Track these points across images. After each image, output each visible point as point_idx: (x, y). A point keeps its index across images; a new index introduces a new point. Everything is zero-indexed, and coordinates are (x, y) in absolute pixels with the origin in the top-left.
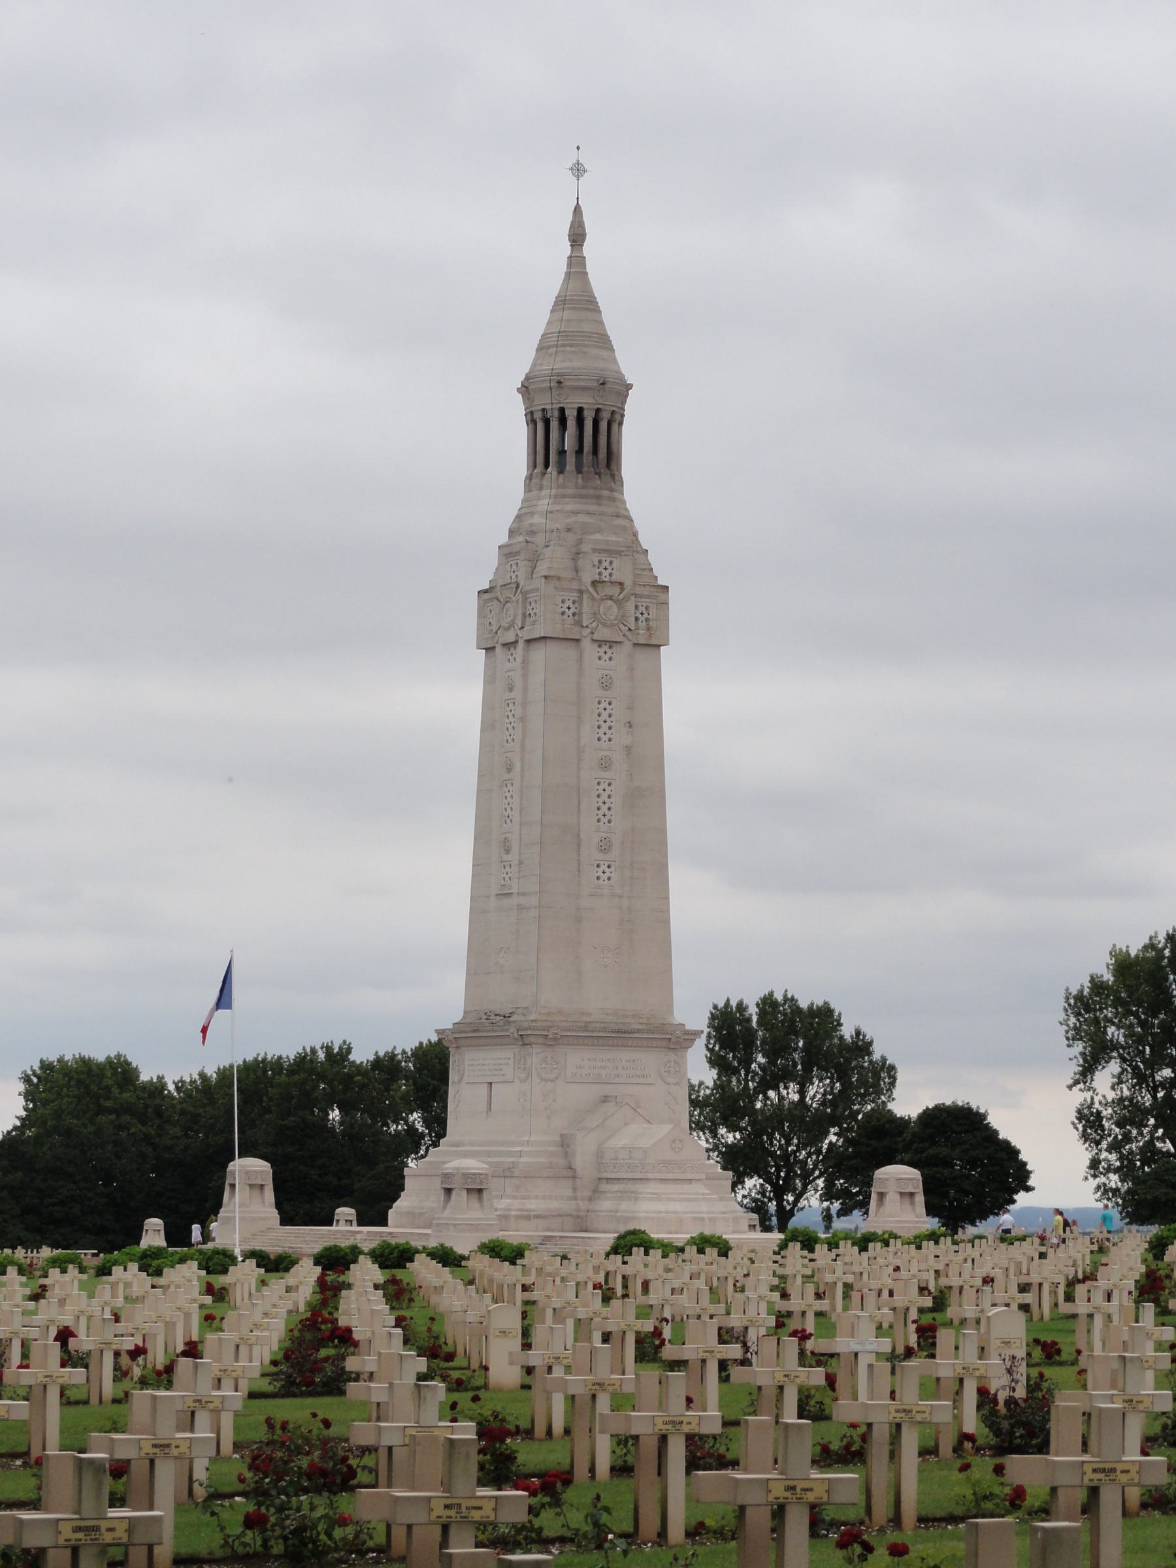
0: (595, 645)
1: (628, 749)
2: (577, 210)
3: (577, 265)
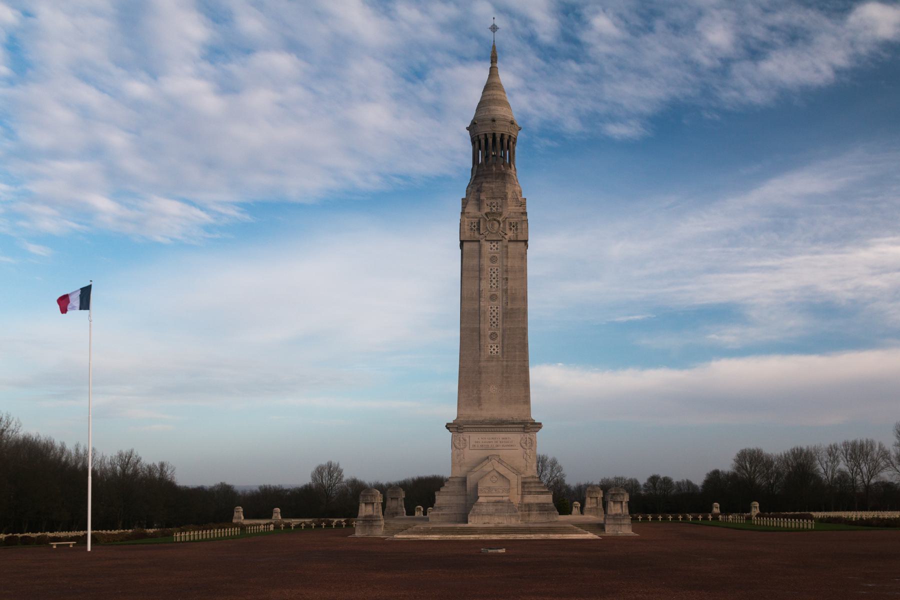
0: (489, 243)
1: (505, 291)
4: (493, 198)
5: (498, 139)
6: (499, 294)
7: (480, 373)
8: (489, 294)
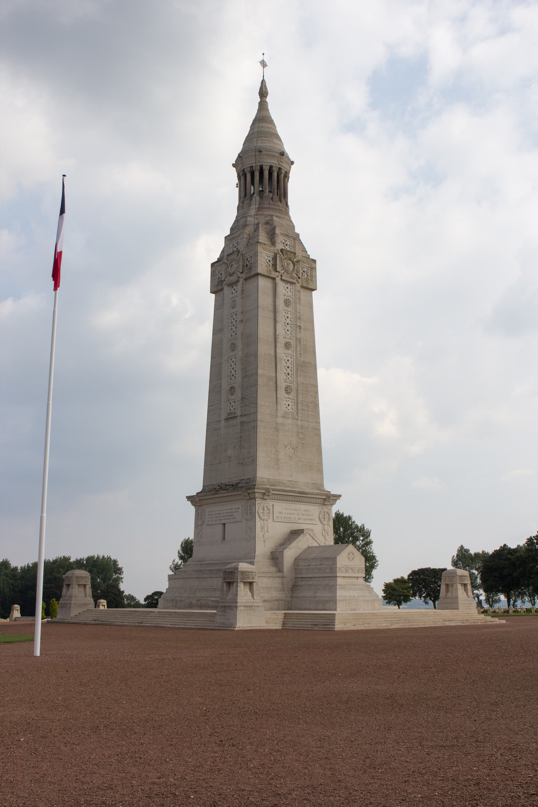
2: (263, 82)
3: (263, 106)
7: (277, 430)
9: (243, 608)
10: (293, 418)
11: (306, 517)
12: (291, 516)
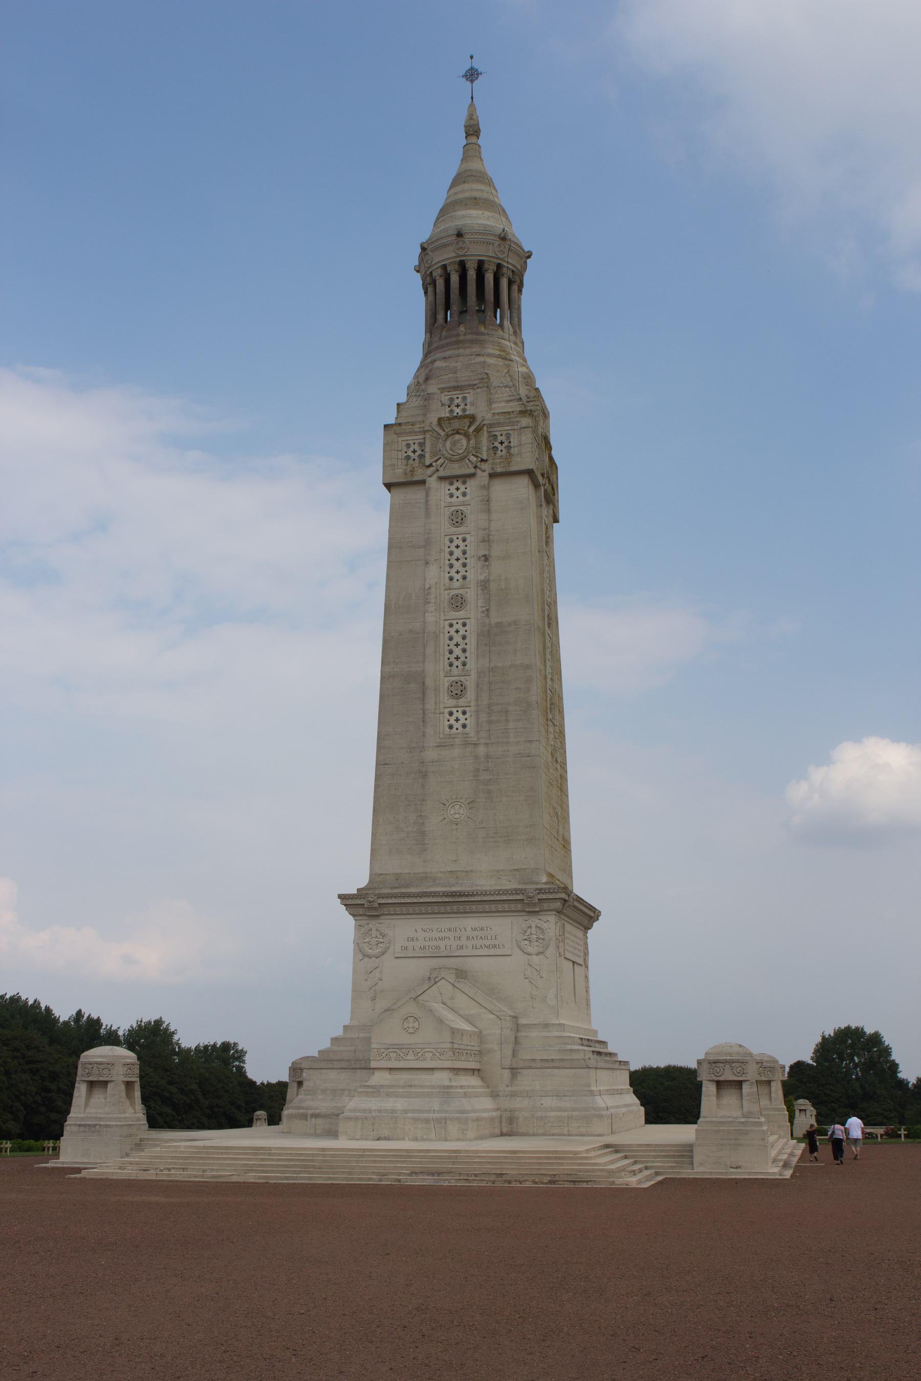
0: (445, 486)
1: (484, 585)
2: (472, 105)
4: (456, 388)
5: (472, 274)
6: (471, 594)
7: (425, 775)
8: (446, 596)
9: (75, 1129)
10: (466, 744)
11: (479, 943)
12: (439, 943)
